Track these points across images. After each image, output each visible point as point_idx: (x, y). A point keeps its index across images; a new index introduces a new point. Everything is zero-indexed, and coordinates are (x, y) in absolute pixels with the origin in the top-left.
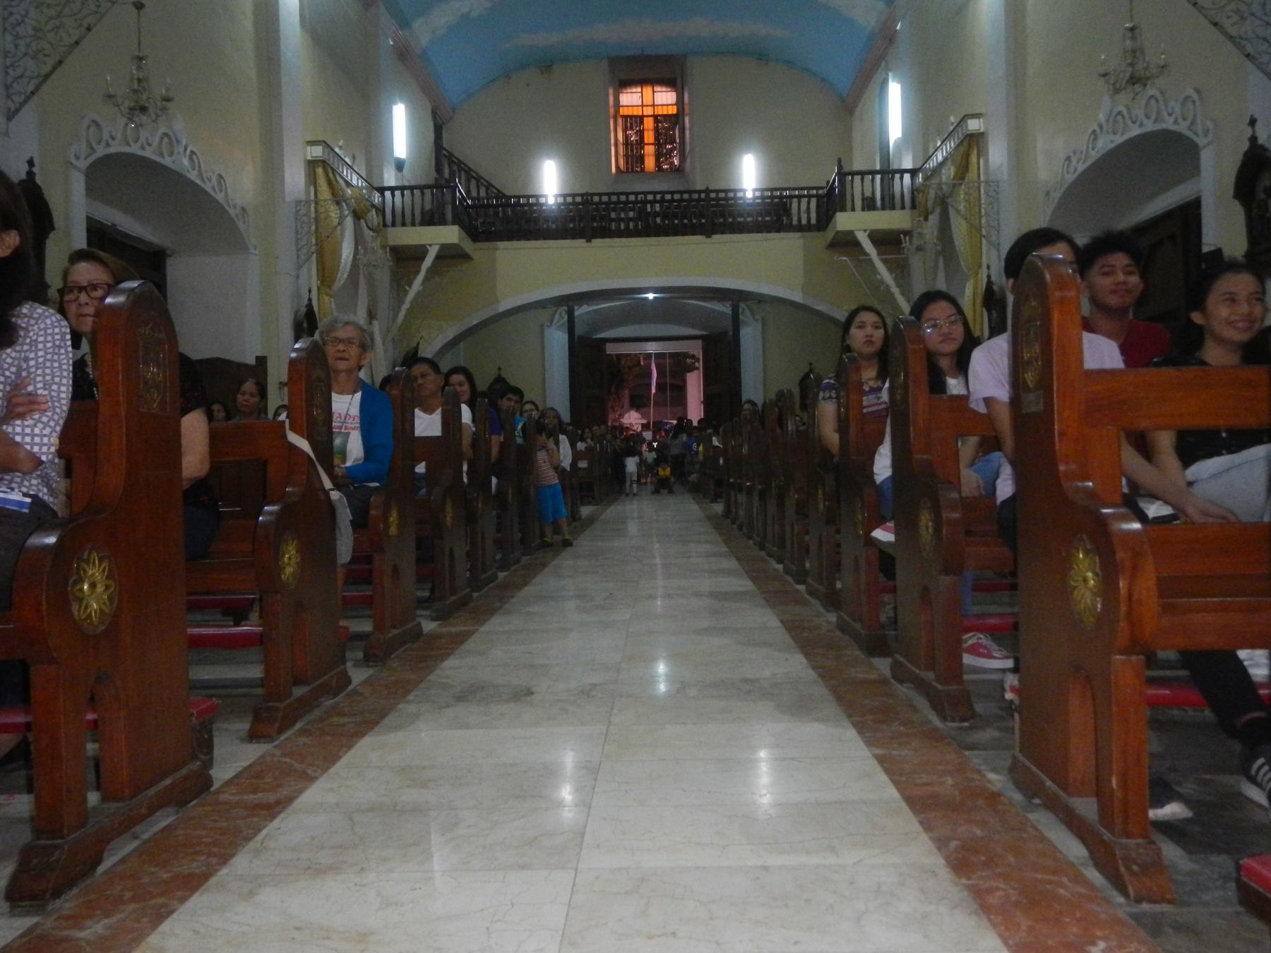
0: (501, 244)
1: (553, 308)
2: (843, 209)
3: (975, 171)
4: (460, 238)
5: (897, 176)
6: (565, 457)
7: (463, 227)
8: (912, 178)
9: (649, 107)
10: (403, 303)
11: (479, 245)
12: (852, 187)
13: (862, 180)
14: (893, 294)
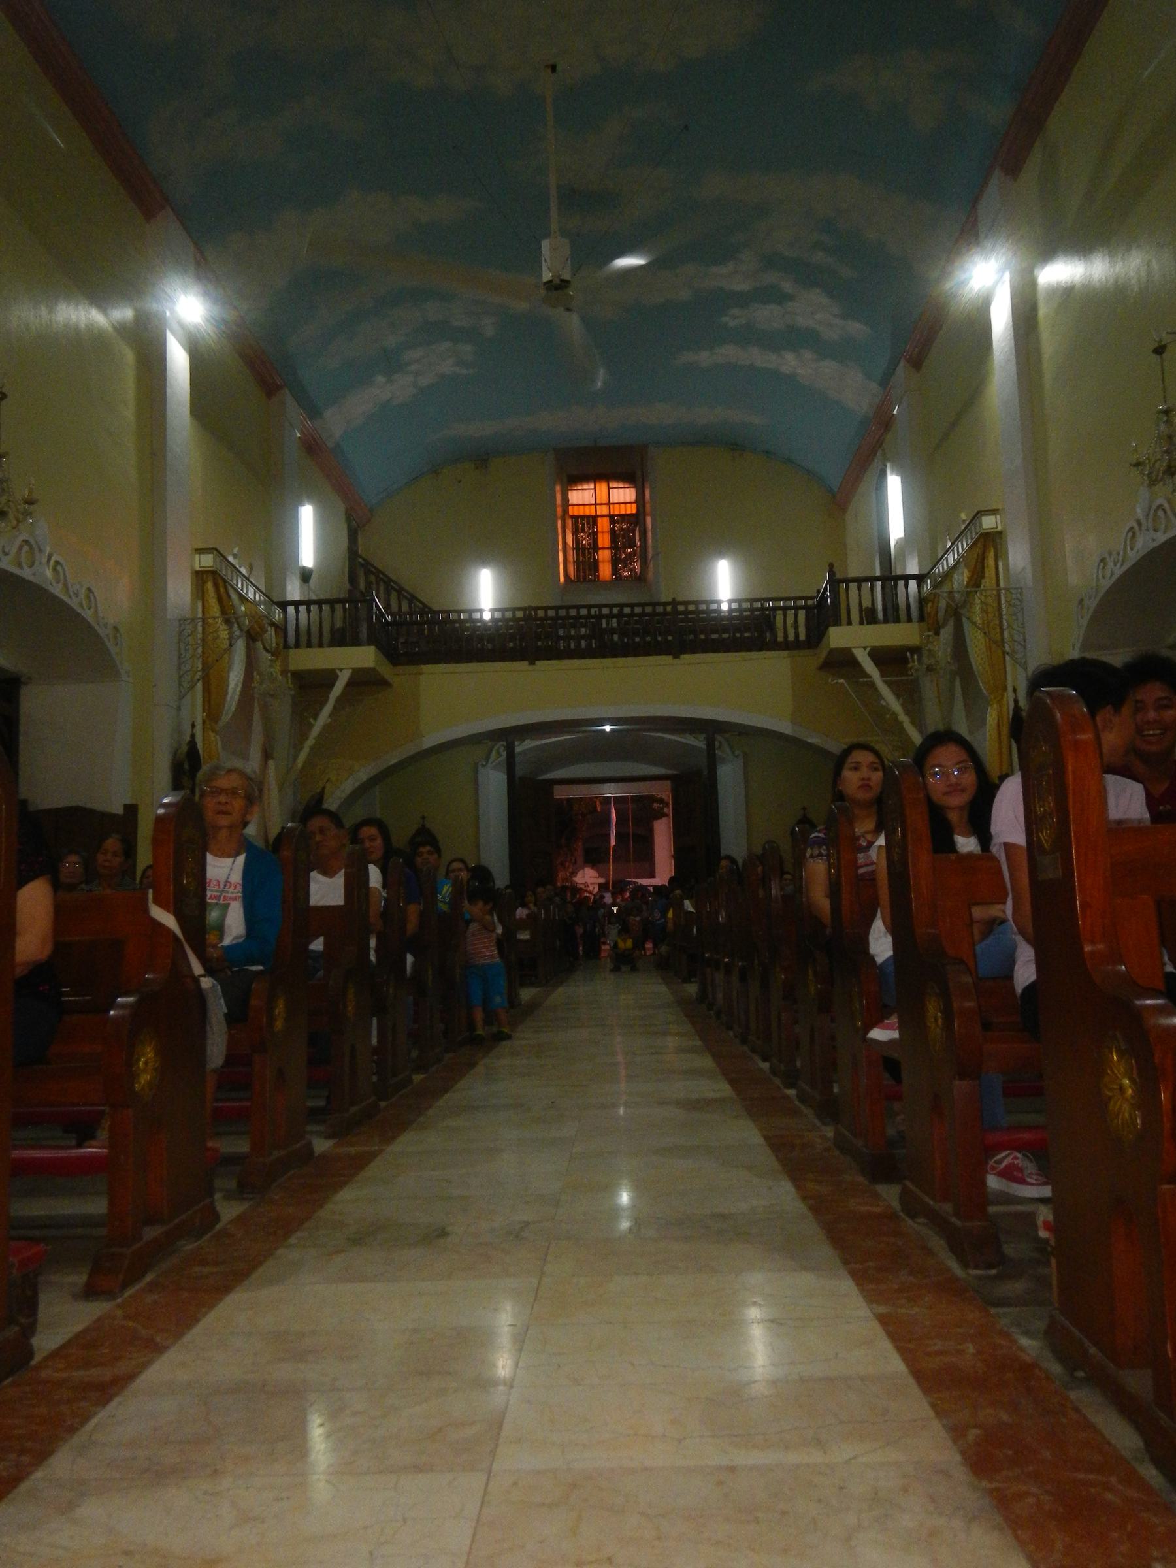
0: (424, 668)
2: (837, 623)
5: (901, 583)
7: (380, 647)
8: (919, 586)
9: (604, 506)
10: (307, 739)
13: (859, 589)
14: (901, 723)
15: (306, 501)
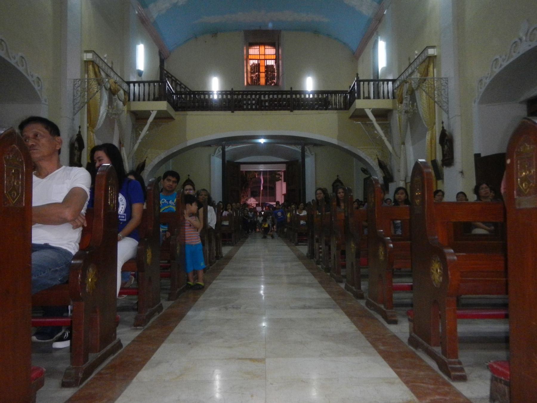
2: (359, 97)
3: (432, 75)
4: (167, 107)
5: (385, 83)
6: (211, 221)
8: (393, 84)
12: (364, 87)
13: (369, 84)
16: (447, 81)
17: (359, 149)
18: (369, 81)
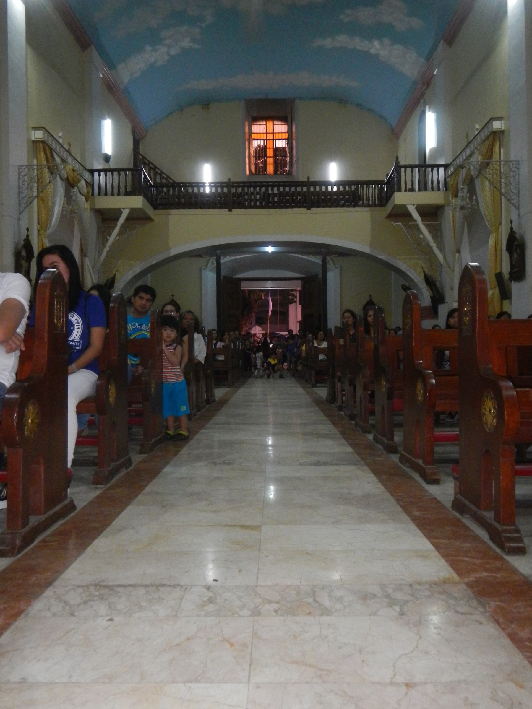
0: (173, 211)
1: (208, 258)
2: (399, 190)
3: (498, 156)
4: (143, 204)
5: (435, 169)
6: (200, 352)
8: (445, 170)
9: (270, 134)
10: (105, 247)
11: (158, 212)
12: (405, 176)
13: (412, 171)
14: (432, 247)
15: (108, 118)
16: (518, 164)
17: (399, 259)
18: (412, 167)
